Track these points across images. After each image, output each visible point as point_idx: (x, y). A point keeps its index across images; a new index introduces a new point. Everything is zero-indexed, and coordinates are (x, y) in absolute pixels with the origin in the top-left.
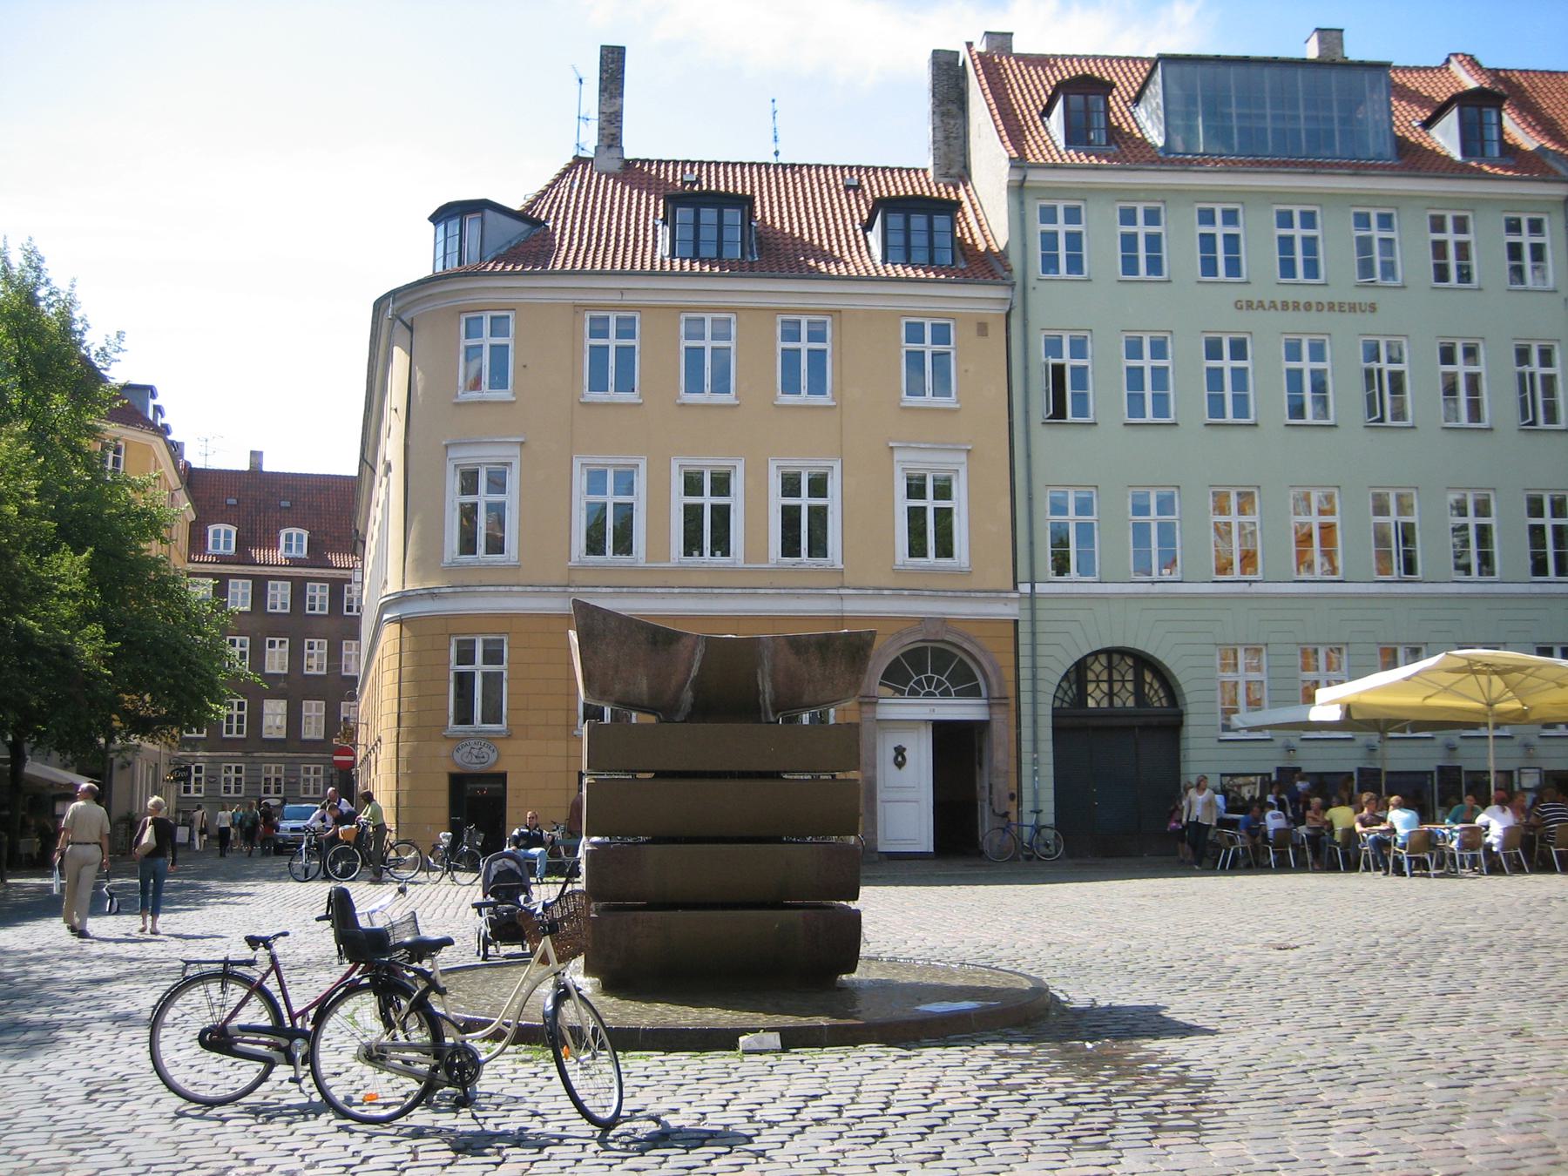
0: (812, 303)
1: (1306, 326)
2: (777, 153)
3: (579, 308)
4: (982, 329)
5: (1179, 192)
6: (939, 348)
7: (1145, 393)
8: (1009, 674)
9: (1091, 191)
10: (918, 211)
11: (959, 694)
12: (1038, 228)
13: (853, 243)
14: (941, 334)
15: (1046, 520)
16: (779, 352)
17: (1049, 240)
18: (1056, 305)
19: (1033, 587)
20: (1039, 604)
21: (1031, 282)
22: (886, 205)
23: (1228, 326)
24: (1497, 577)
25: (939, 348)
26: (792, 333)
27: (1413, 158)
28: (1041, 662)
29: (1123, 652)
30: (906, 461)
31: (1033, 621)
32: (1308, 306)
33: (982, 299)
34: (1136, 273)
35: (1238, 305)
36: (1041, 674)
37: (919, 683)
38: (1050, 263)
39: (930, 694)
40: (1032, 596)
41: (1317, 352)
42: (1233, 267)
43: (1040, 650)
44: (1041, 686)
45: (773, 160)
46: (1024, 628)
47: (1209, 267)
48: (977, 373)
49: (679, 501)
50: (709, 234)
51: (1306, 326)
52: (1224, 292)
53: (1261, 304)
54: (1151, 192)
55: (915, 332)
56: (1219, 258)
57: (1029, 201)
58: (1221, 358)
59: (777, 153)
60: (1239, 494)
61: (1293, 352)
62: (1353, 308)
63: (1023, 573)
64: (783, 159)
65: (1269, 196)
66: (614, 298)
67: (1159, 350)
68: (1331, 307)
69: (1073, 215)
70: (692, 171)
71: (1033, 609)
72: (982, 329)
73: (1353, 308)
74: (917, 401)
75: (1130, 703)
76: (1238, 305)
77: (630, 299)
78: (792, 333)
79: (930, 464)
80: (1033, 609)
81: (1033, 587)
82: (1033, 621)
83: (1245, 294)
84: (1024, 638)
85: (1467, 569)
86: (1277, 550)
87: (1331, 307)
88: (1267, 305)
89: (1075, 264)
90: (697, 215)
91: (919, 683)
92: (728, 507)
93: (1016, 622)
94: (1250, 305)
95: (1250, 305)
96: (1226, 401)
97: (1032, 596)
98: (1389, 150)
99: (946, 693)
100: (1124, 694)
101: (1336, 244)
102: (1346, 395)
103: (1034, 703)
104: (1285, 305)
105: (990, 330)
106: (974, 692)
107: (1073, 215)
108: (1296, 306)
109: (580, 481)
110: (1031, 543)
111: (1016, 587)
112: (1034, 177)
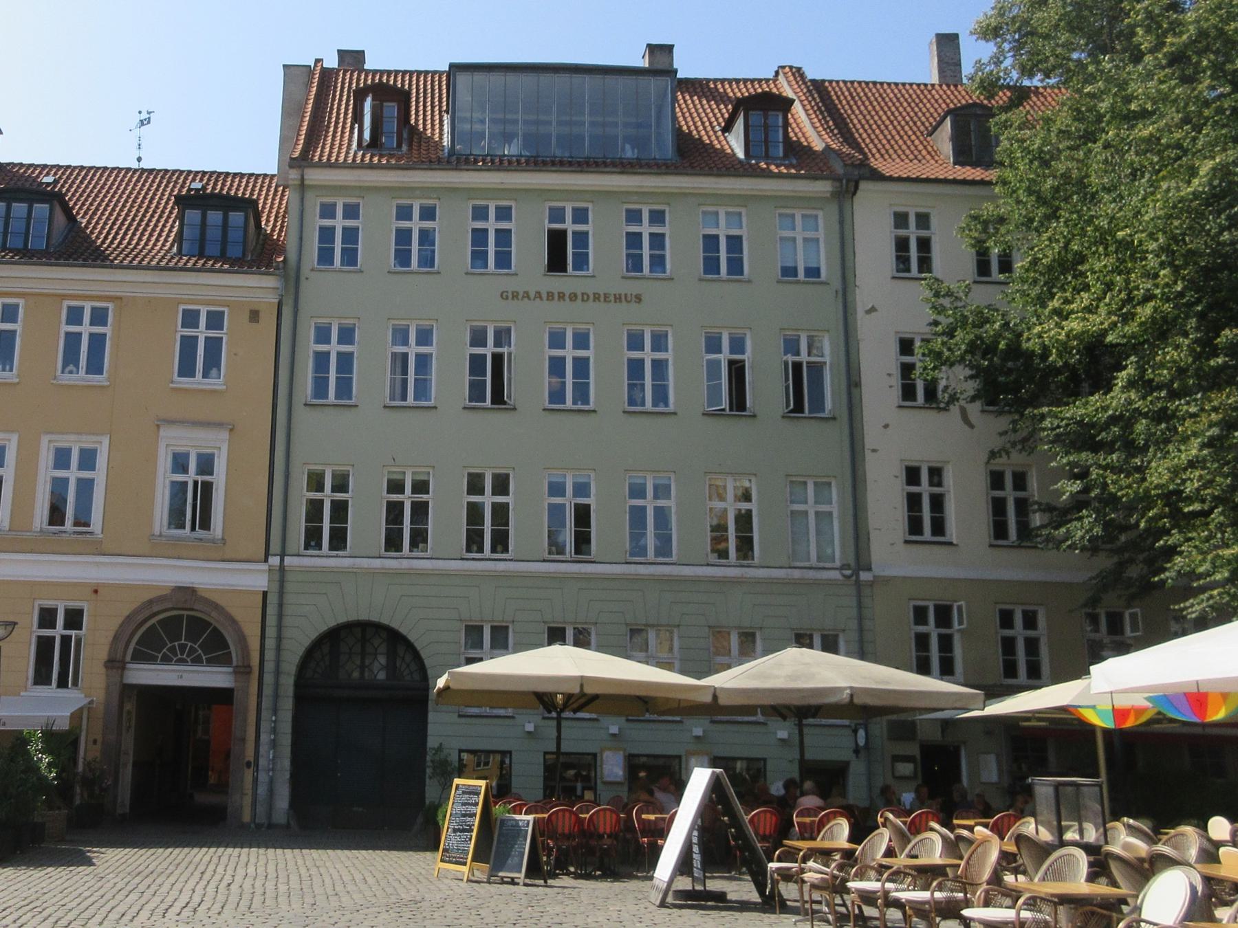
0: (95, 290)
1: (569, 318)
2: (139, 159)
4: (254, 316)
5: (453, 190)
6: (213, 334)
7: (410, 379)
8: (254, 644)
9: (369, 189)
10: (216, 208)
11: (210, 662)
12: (317, 222)
13: (156, 234)
14: (215, 321)
16: (62, 335)
17: (327, 234)
18: (327, 295)
19: (282, 560)
20: (289, 577)
21: (305, 271)
22: (185, 202)
24: (674, 558)
25: (213, 334)
26: (75, 316)
27: (693, 155)
28: (287, 633)
29: (378, 627)
30: (173, 439)
31: (281, 593)
32: (573, 297)
33: (258, 287)
34: (409, 265)
35: (503, 296)
36: (286, 644)
37: (172, 650)
38: (326, 256)
39: (181, 661)
40: (282, 567)
41: (581, 341)
42: (503, 260)
43: (287, 621)
44: (286, 655)
45: (135, 165)
46: (273, 599)
47: (479, 256)
48: (247, 356)
50: (214, 233)
51: (569, 318)
52: (491, 283)
53: (526, 295)
54: (426, 191)
55: (190, 319)
56: (491, 251)
57: (309, 195)
58: (80, 334)
59: (139, 159)
60: (816, 484)
61: (557, 340)
62: (618, 298)
63: (275, 546)
64: (145, 165)
67: (347, 335)
68: (597, 297)
69: (351, 212)
70: (201, 180)
71: (282, 582)
72: (254, 316)
73: (618, 298)
74: (186, 382)
75: (382, 676)
76: (503, 296)
78: (75, 316)
79: (193, 442)
80: (282, 582)
81: (282, 560)
82: (281, 593)
83: (511, 284)
84: (272, 610)
85: (723, 554)
86: (690, 535)
87: (597, 297)
88: (532, 295)
89: (350, 257)
90: (204, 217)
91: (172, 650)
92: (93, 480)
93: (265, 594)
94: (515, 295)
95: (515, 295)
96: (491, 384)
97: (282, 567)
98: (669, 151)
99: (197, 661)
100: (376, 666)
101: (604, 239)
102: (608, 383)
103: (277, 672)
104: (550, 296)
105: (263, 316)
106: (225, 660)
107: (351, 212)
108: (561, 296)
109: (164, 462)
110: (285, 519)
111: (266, 561)
112: (315, 176)
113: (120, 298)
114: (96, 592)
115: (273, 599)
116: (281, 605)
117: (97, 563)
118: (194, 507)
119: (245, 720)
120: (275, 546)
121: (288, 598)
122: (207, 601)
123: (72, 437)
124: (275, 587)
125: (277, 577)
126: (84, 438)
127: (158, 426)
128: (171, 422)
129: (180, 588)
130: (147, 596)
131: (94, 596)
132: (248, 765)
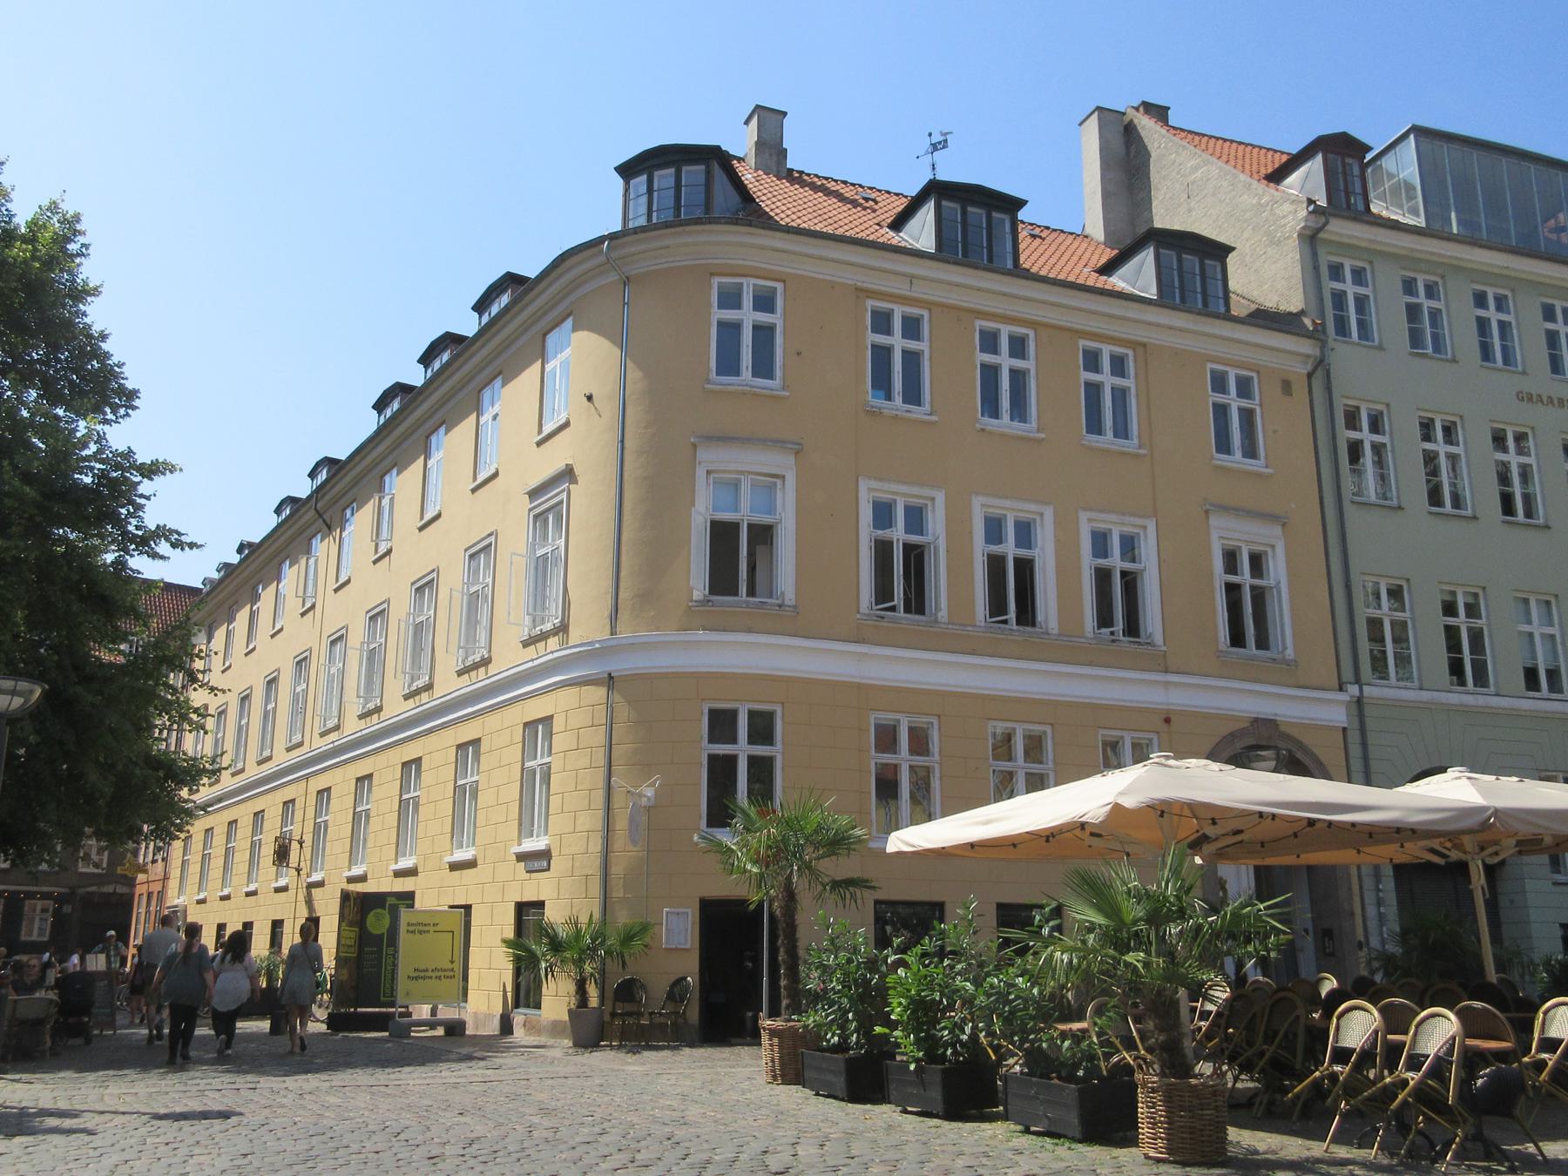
3: (864, 292)
15: (1363, 612)
20: (1368, 711)
23: (1514, 418)
30: (1224, 531)
35: (1520, 397)
40: (1359, 701)
49: (980, 549)
65: (1535, 285)
66: (901, 288)
72: (1287, 386)
76: (1520, 397)
77: (919, 291)
79: (1247, 534)
81: (1361, 690)
93: (1344, 729)
97: (1359, 701)
113: (1144, 345)
114: (1167, 721)
115: (1354, 737)
116: (1364, 745)
117: (1167, 683)
118: (1247, 618)
119: (1350, 889)
120: (1348, 674)
121: (1372, 739)
122: (1289, 738)
123: (1113, 517)
124: (1356, 724)
125: (1354, 711)
126: (1127, 519)
127: (1207, 512)
128: (1225, 509)
129: (1256, 720)
130: (1225, 730)
131: (1165, 726)
132: (1360, 945)
